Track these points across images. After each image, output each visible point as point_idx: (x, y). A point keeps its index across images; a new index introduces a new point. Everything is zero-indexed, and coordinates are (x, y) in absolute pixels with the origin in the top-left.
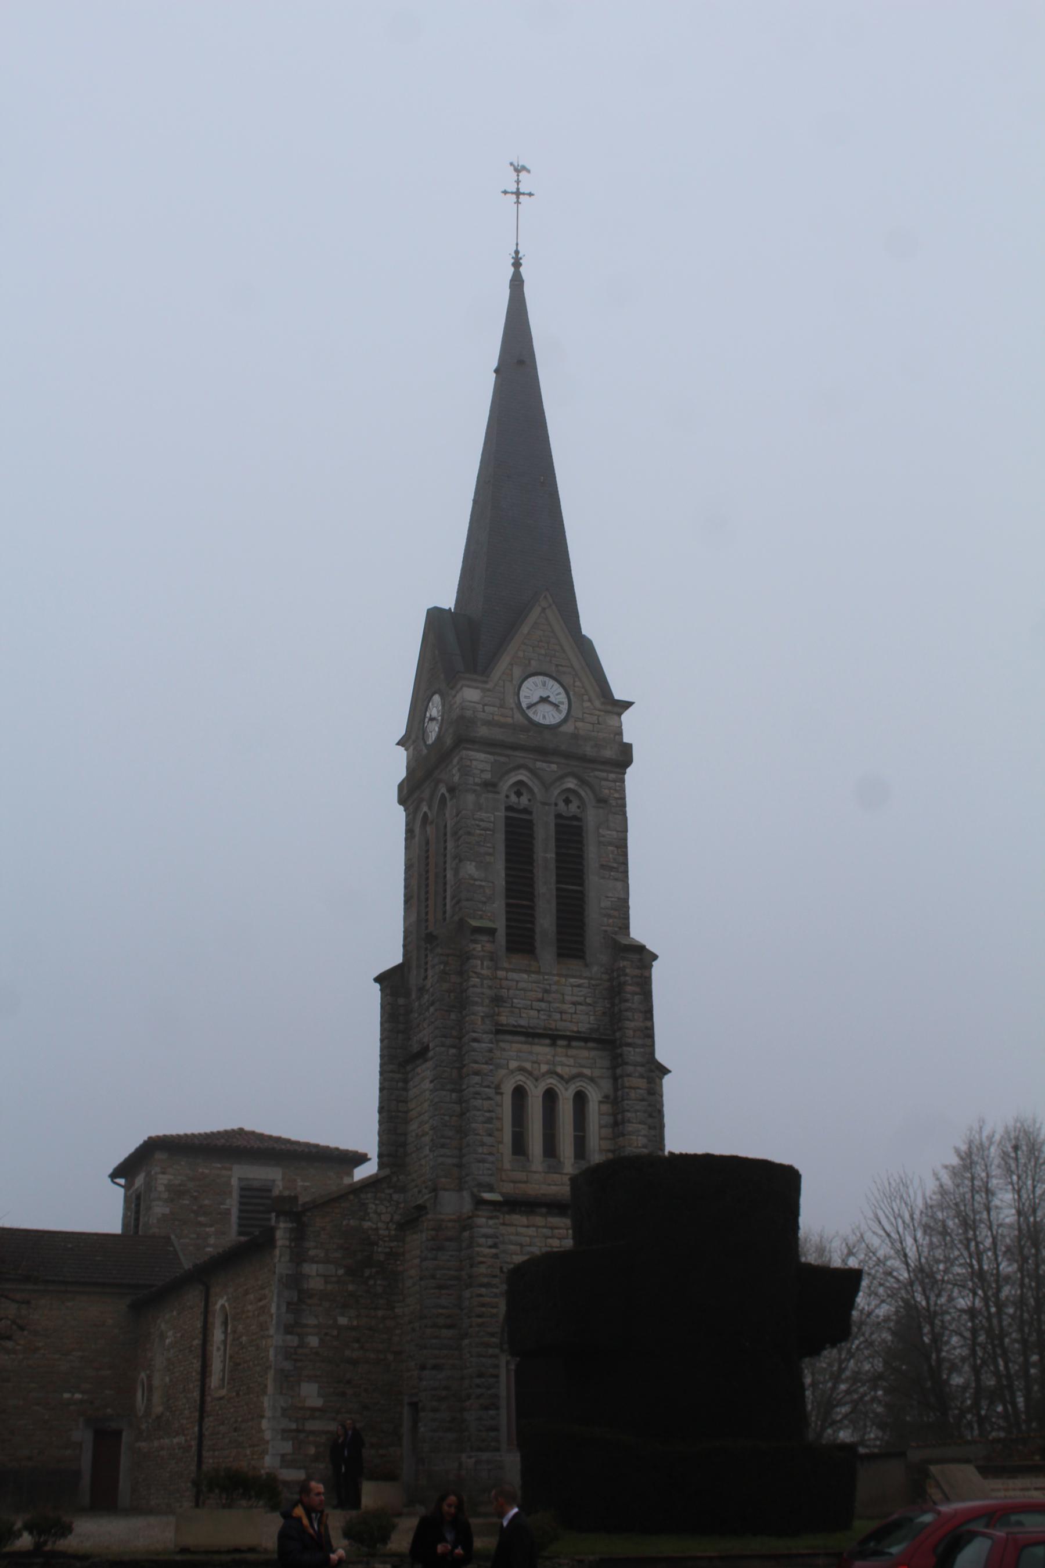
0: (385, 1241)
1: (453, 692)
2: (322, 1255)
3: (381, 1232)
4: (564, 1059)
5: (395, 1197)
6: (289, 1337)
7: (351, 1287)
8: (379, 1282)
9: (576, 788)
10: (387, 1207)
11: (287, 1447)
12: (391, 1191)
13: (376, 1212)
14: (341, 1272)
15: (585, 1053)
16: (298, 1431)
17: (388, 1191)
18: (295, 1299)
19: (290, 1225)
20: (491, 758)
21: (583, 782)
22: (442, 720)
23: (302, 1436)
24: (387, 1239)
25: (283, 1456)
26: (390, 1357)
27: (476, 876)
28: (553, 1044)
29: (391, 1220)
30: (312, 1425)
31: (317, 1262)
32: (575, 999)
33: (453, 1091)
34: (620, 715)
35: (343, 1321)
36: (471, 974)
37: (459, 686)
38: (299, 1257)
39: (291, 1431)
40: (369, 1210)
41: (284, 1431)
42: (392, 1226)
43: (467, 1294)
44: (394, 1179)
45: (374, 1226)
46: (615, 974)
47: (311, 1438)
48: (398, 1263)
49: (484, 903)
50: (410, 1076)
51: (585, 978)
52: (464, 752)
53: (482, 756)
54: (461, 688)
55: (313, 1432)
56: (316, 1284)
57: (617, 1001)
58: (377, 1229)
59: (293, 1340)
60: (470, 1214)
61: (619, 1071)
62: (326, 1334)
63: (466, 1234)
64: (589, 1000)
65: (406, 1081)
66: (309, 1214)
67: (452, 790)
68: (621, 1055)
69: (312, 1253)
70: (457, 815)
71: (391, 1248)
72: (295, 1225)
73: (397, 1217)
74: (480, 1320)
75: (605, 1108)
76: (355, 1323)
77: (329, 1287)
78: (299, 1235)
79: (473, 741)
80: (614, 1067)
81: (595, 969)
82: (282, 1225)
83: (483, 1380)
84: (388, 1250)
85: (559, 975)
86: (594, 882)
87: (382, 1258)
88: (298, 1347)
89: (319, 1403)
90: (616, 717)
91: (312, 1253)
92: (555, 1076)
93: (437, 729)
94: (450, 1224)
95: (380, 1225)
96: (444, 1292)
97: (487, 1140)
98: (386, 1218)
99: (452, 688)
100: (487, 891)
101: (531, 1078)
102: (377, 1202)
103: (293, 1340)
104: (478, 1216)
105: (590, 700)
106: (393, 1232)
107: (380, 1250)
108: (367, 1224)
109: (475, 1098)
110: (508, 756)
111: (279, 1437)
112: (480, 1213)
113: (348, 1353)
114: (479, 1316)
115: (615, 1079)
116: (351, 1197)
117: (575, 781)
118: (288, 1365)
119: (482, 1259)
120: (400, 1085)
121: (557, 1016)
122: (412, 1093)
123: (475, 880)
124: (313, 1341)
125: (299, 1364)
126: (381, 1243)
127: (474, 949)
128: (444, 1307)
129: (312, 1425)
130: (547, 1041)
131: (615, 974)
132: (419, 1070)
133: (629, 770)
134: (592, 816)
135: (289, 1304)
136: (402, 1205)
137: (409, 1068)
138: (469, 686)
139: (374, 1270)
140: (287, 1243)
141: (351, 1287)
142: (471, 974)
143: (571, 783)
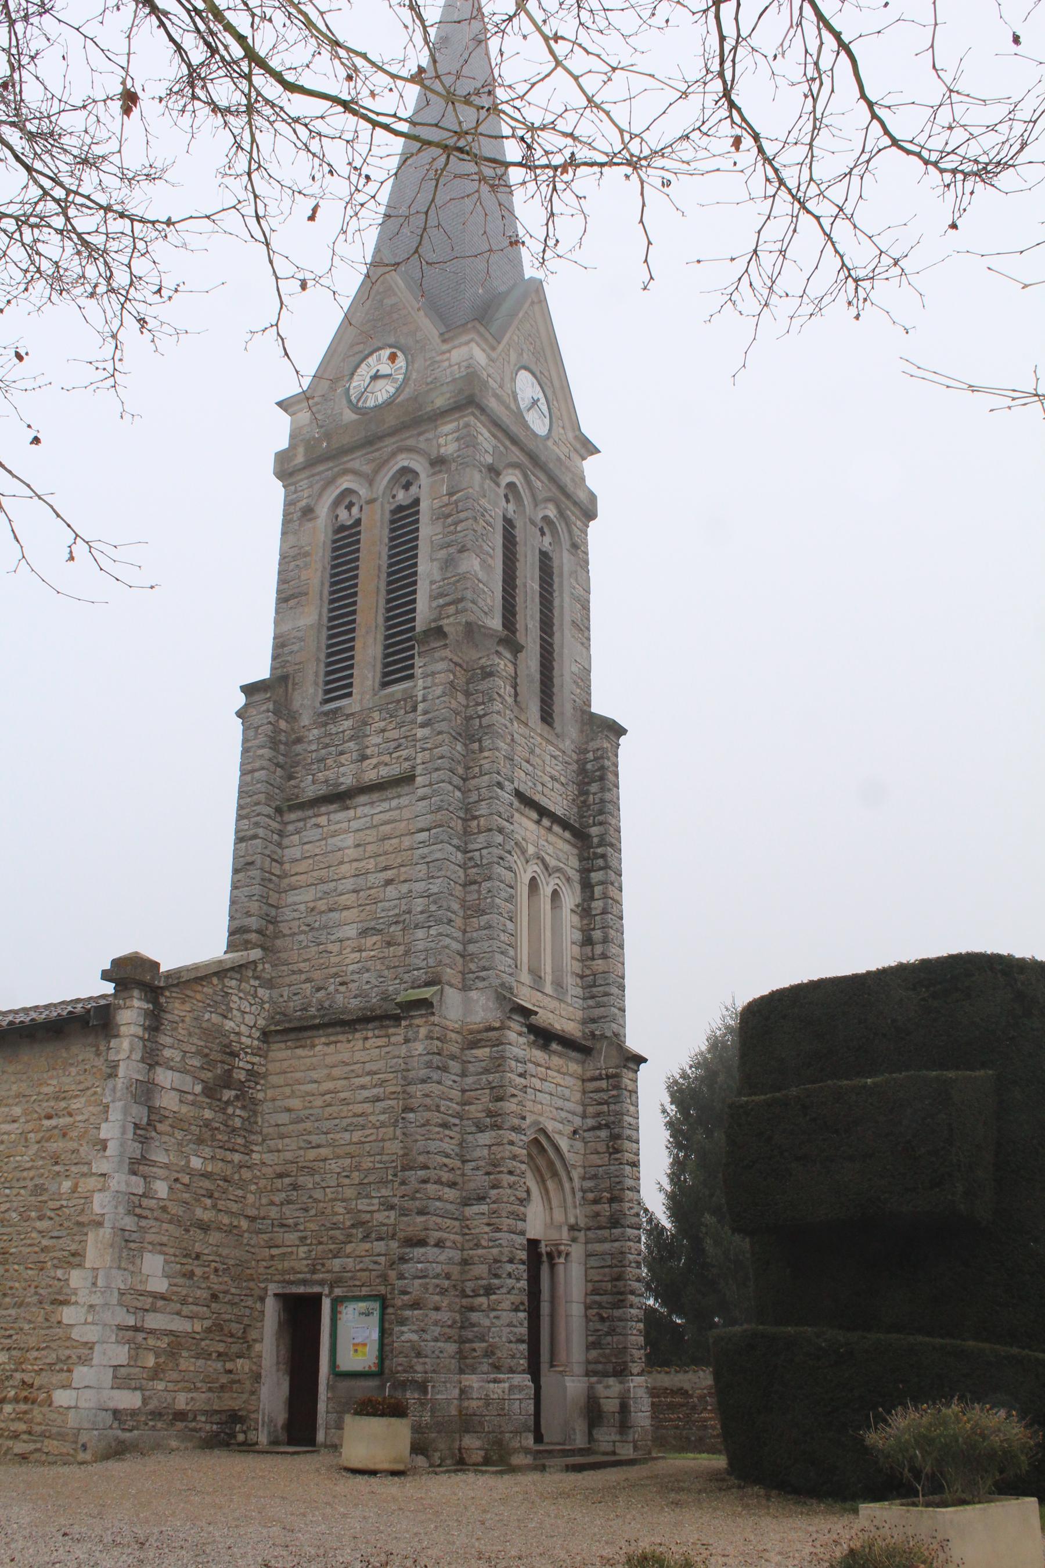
0: (246, 1053)
1: (445, 347)
2: (178, 1059)
3: (244, 1039)
4: (546, 844)
5: (261, 992)
6: (134, 1178)
7: (208, 1114)
8: (238, 1112)
9: (555, 520)
10: (251, 1005)
11: (121, 1354)
12: (257, 983)
13: (239, 1010)
14: (198, 1088)
15: (560, 844)
16: (136, 1329)
17: (252, 982)
18: (145, 1120)
19: (145, 1006)
20: (494, 442)
21: (561, 513)
22: (406, 380)
23: (140, 1336)
24: (249, 1050)
25: (116, 1367)
26: (244, 1224)
27: (480, 576)
28: (538, 822)
29: (254, 1026)
30: (154, 1321)
31: (171, 1069)
32: (554, 772)
33: (458, 848)
34: (584, 459)
35: (196, 1163)
36: (496, 696)
37: (465, 338)
38: (152, 1059)
39: (128, 1328)
40: (232, 1005)
41: (120, 1328)
42: (257, 1034)
43: (485, 1138)
44: (260, 967)
45: (237, 1029)
46: (590, 755)
47: (151, 1342)
48: (259, 1087)
49: (486, 613)
50: (290, 828)
51: (560, 750)
52: (472, 420)
53: (487, 434)
54: (467, 343)
55: (152, 1332)
56: (168, 1101)
57: (594, 788)
58: (238, 1034)
59: (137, 1185)
60: (497, 1025)
61: (596, 877)
62: (176, 1180)
63: (482, 1052)
64: (563, 779)
65: (281, 834)
66: (167, 994)
67: (438, 463)
68: (603, 856)
69: (167, 1053)
70: (451, 494)
71: (253, 1064)
72: (151, 1006)
73: (261, 1022)
74: (512, 1178)
75: (576, 919)
76: (209, 1169)
77: (184, 1109)
78: (154, 1022)
79: (483, 410)
80: (585, 872)
81: (568, 743)
82: (136, 1003)
83: (514, 1266)
84: (249, 1067)
85: (541, 735)
86: (565, 638)
87: (242, 1076)
88: (144, 1195)
89: (159, 1285)
90: (579, 458)
91: (167, 1053)
92: (539, 862)
93: (392, 390)
94: (453, 1035)
95: (244, 1029)
96: (447, 1132)
97: (510, 925)
98: (249, 1019)
99: (444, 341)
100: (489, 601)
101: (522, 858)
102: (241, 995)
103: (137, 1185)
104: (509, 1028)
105: (563, 428)
106: (256, 1043)
107: (241, 1064)
108: (229, 1025)
109: (499, 864)
110: (506, 448)
111: (113, 1339)
112: (512, 1024)
113: (199, 1213)
114: (511, 1173)
115: (587, 886)
116: (215, 981)
117: (555, 512)
118: (129, 1223)
119: (515, 1092)
120: (276, 837)
121: (540, 788)
122: (295, 852)
123: (479, 580)
124: (161, 1189)
125: (143, 1223)
126: (242, 1055)
127: (499, 664)
128: (447, 1156)
129: (154, 1321)
130: (535, 816)
131: (590, 755)
132: (323, 820)
133: (591, 523)
134: (564, 561)
135: (136, 1126)
136: (266, 1006)
137: (293, 816)
138: (478, 345)
139: (233, 1093)
140: (140, 1031)
141: (208, 1114)
142: (496, 696)
143: (551, 512)
